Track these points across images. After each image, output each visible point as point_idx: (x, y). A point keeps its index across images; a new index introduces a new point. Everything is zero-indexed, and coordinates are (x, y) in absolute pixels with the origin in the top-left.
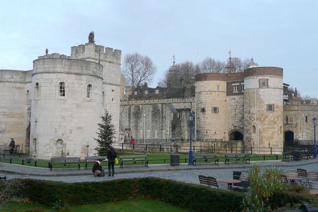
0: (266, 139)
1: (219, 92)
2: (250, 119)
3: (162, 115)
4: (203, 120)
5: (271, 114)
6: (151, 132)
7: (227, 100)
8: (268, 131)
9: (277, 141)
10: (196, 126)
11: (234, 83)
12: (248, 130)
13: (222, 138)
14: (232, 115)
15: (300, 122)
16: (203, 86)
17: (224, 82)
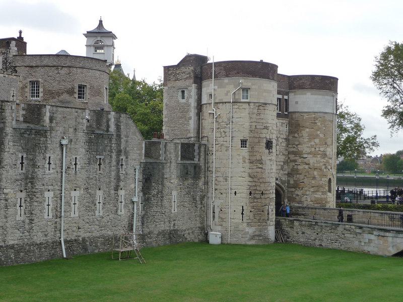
3: (119, 145)
6: (81, 198)
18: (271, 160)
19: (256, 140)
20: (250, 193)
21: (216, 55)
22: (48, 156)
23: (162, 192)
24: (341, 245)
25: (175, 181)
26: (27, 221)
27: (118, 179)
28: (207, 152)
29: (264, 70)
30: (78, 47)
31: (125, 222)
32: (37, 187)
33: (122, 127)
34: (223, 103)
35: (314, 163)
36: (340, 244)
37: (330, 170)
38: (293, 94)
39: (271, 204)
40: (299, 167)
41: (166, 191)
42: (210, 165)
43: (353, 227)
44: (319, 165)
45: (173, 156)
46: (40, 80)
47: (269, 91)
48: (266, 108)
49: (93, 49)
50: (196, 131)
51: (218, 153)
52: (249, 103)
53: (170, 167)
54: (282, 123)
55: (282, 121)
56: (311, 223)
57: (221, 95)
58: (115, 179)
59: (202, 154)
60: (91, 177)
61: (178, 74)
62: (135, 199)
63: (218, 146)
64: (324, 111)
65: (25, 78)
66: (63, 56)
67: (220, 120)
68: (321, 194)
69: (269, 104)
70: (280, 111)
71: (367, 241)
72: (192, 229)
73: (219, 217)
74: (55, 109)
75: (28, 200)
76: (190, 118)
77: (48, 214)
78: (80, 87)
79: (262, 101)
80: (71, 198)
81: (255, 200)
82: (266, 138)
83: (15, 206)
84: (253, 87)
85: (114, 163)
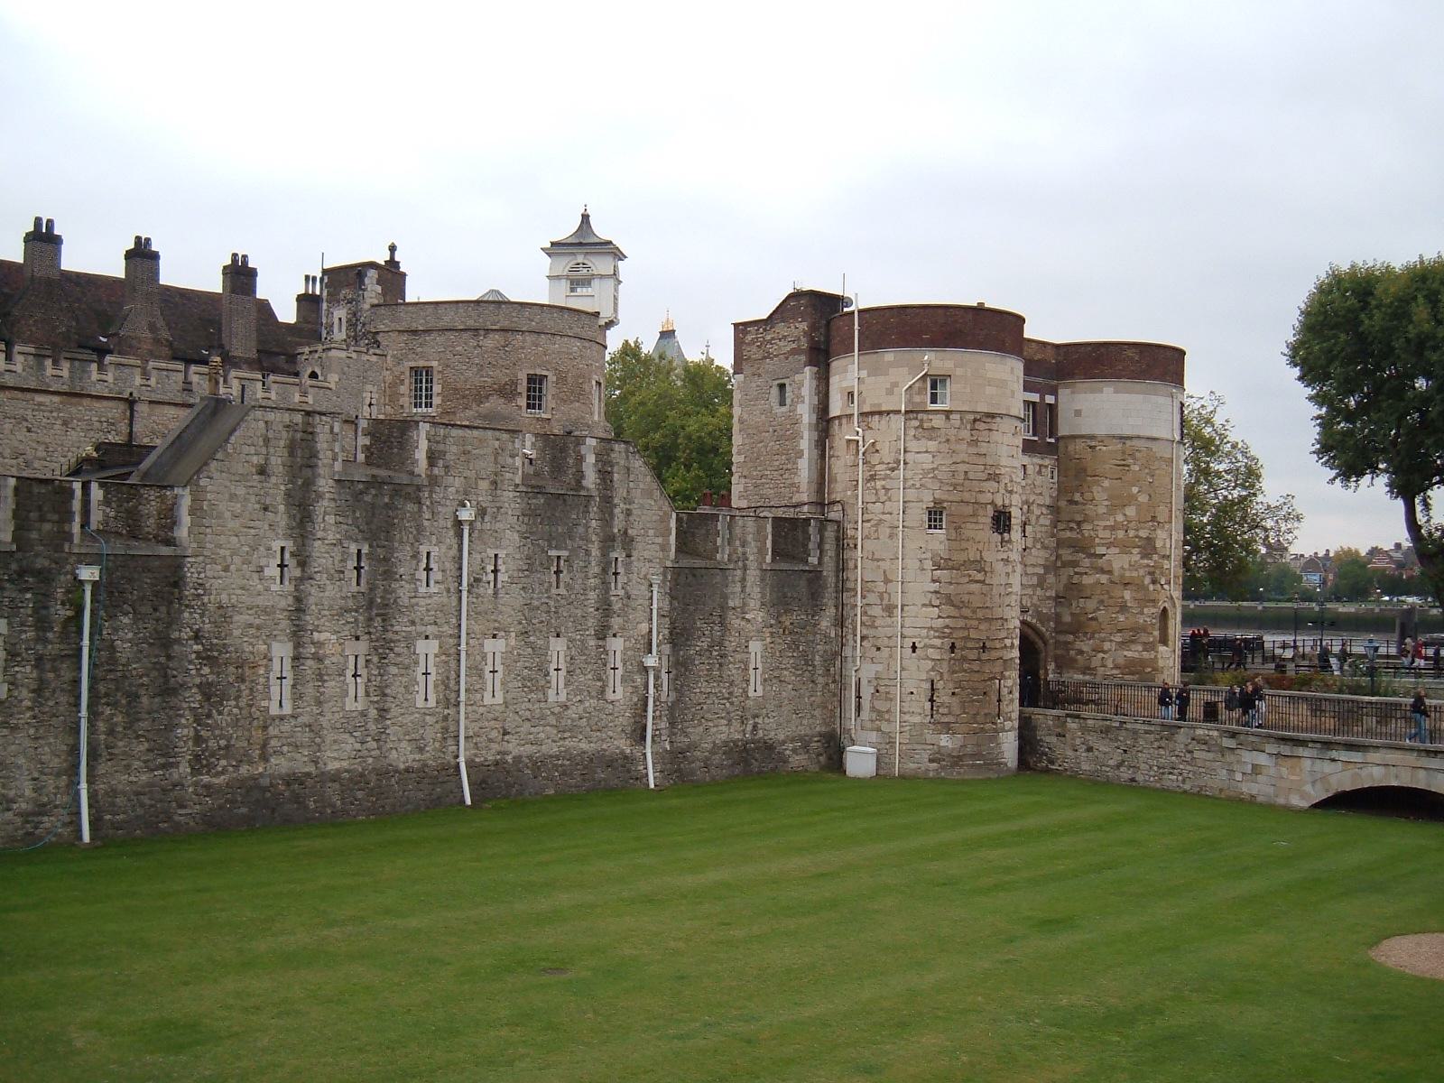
6: (510, 660)
18: (1006, 561)
19: (969, 510)
20: (953, 647)
21: (869, 289)
22: (423, 549)
23: (721, 644)
24: (1184, 781)
25: (757, 615)
26: (373, 713)
27: (605, 608)
28: (842, 543)
29: (988, 329)
30: (531, 281)
31: (625, 719)
32: (397, 628)
33: (616, 476)
34: (880, 413)
35: (1122, 568)
36: (1180, 778)
37: (1165, 586)
38: (1068, 391)
39: (1007, 674)
40: (1087, 580)
41: (732, 642)
42: (850, 575)
43: (1216, 733)
44: (1135, 574)
45: (751, 550)
46: (434, 364)
47: (999, 381)
48: (994, 427)
49: (564, 286)
50: (814, 486)
51: (869, 545)
52: (947, 413)
53: (743, 580)
54: (1040, 466)
56: (1108, 723)
57: (876, 396)
58: (597, 610)
59: (830, 547)
60: (536, 603)
61: (769, 342)
62: (651, 661)
63: (868, 525)
64: (1148, 434)
65: (399, 361)
66: (496, 304)
67: (875, 459)
68: (1140, 648)
69: (1001, 416)
70: (1034, 435)
71: (1249, 769)
72: (801, 739)
73: (873, 709)
74: (442, 431)
75: (375, 659)
76: (800, 454)
77: (425, 697)
78: (532, 379)
80: (484, 657)
81: (966, 666)
82: (992, 503)
83: (342, 674)
84: (959, 372)
85: (595, 569)
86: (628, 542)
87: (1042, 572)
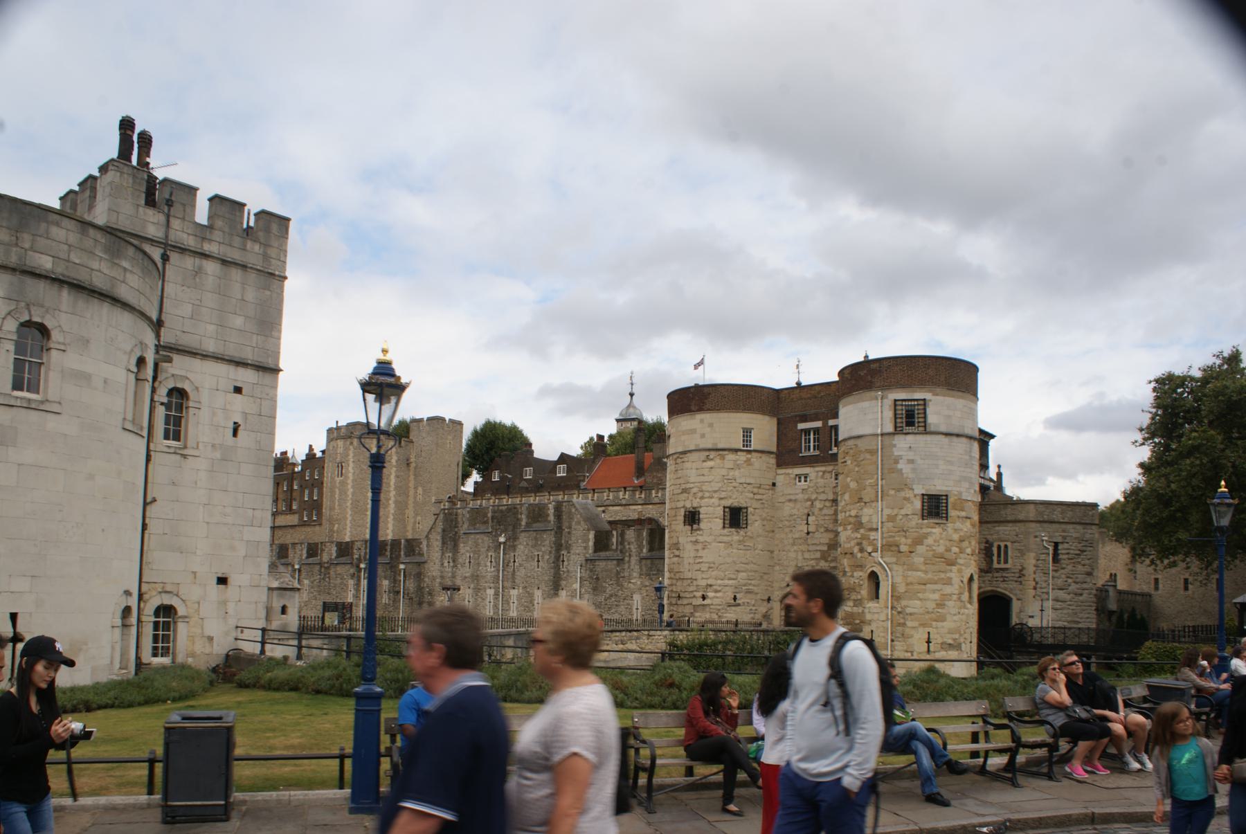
0: (915, 624)
1: (749, 452)
2: (862, 550)
4: (693, 554)
5: (937, 530)
6: (519, 598)
7: (780, 480)
8: (924, 591)
9: (957, 630)
10: (667, 575)
11: (805, 419)
12: (852, 590)
13: (758, 617)
14: (797, 536)
15: (1034, 562)
16: (693, 431)
17: (767, 418)
45: (633, 548)
54: (824, 472)
55: (823, 469)
68: (851, 603)
69: (690, 451)
79: (680, 449)
86: (568, 548)
87: (825, 548)
